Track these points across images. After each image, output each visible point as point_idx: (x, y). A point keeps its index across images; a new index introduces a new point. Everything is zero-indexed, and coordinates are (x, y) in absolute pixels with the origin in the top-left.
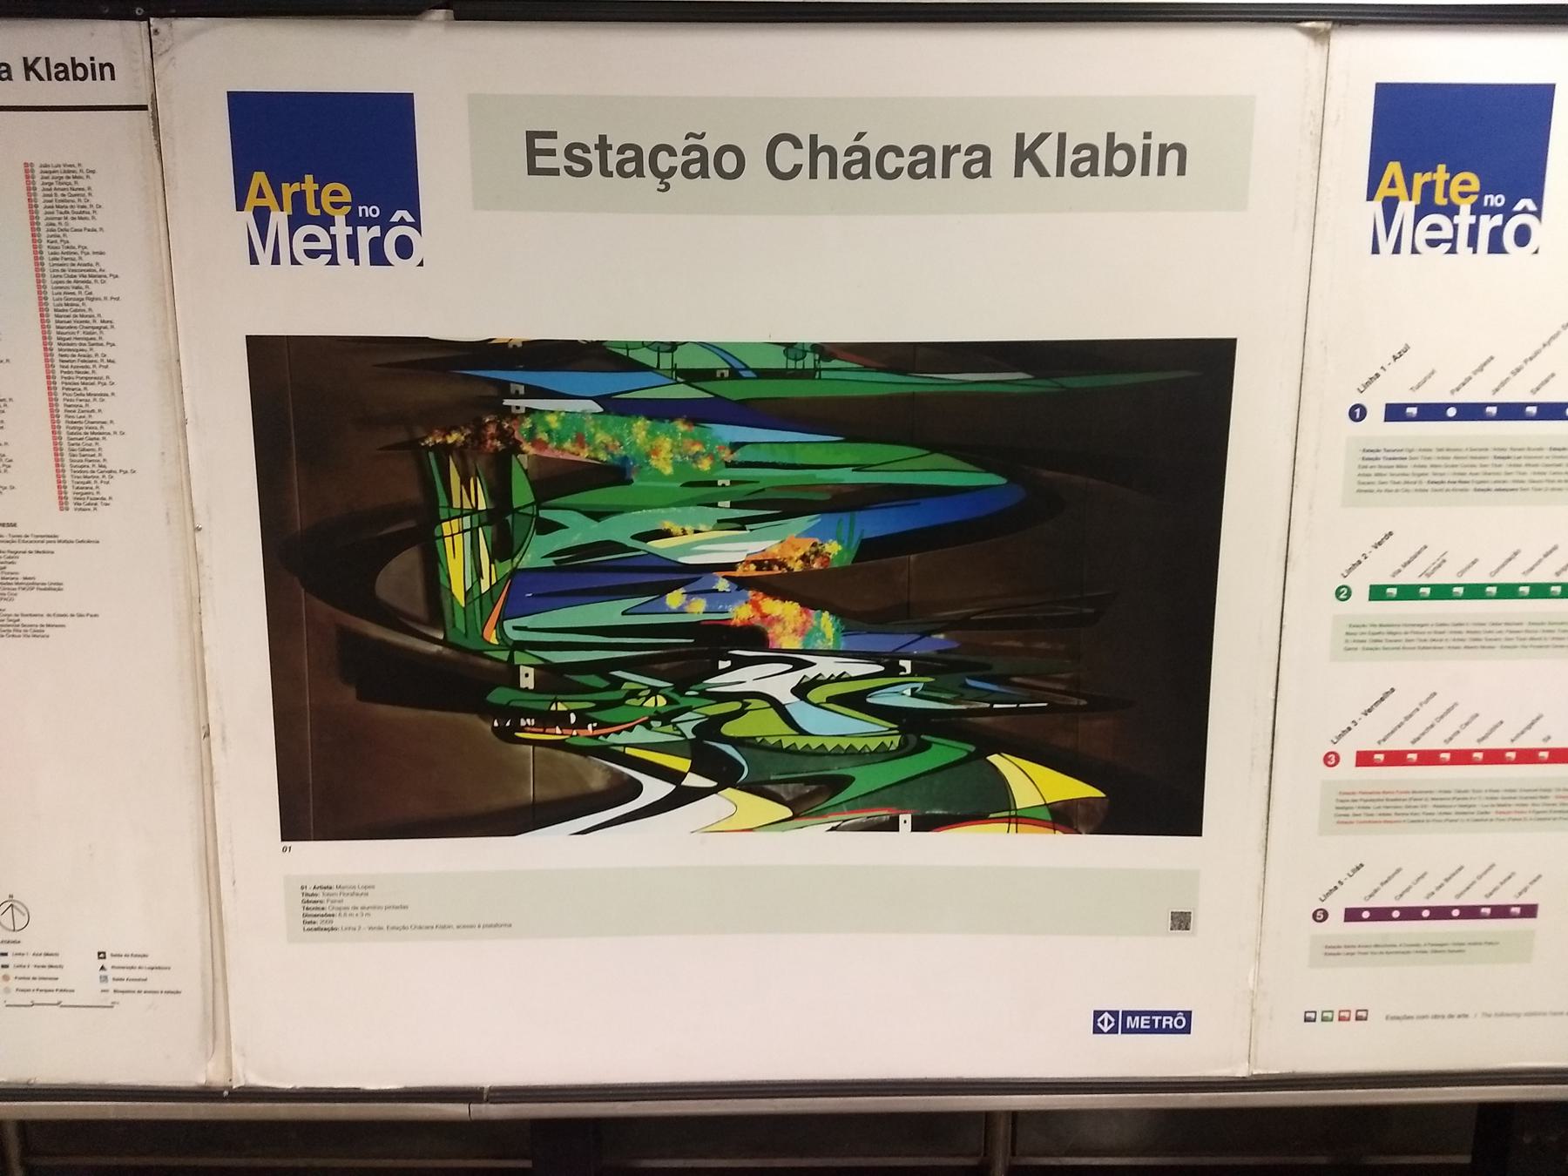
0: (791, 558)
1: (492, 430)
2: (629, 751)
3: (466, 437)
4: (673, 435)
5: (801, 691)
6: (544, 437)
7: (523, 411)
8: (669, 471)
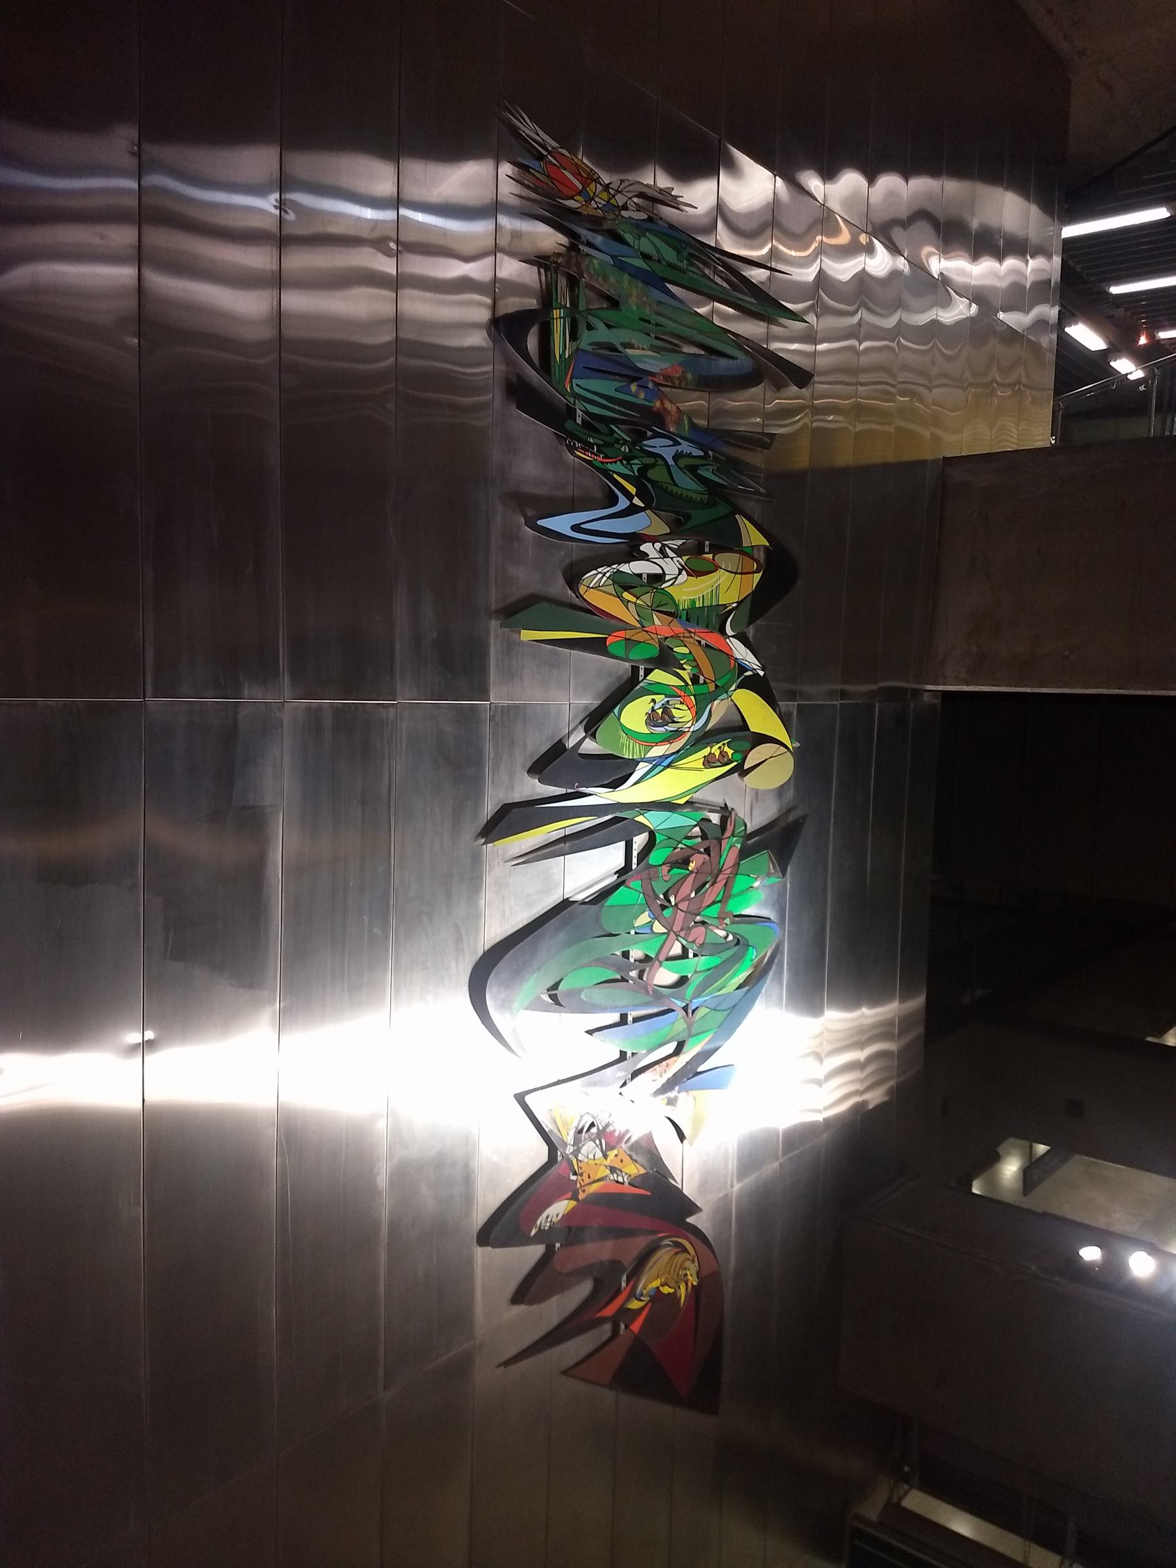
0: (674, 377)
1: (574, 260)
2: (615, 476)
5: (676, 457)
6: (592, 271)
7: (585, 253)
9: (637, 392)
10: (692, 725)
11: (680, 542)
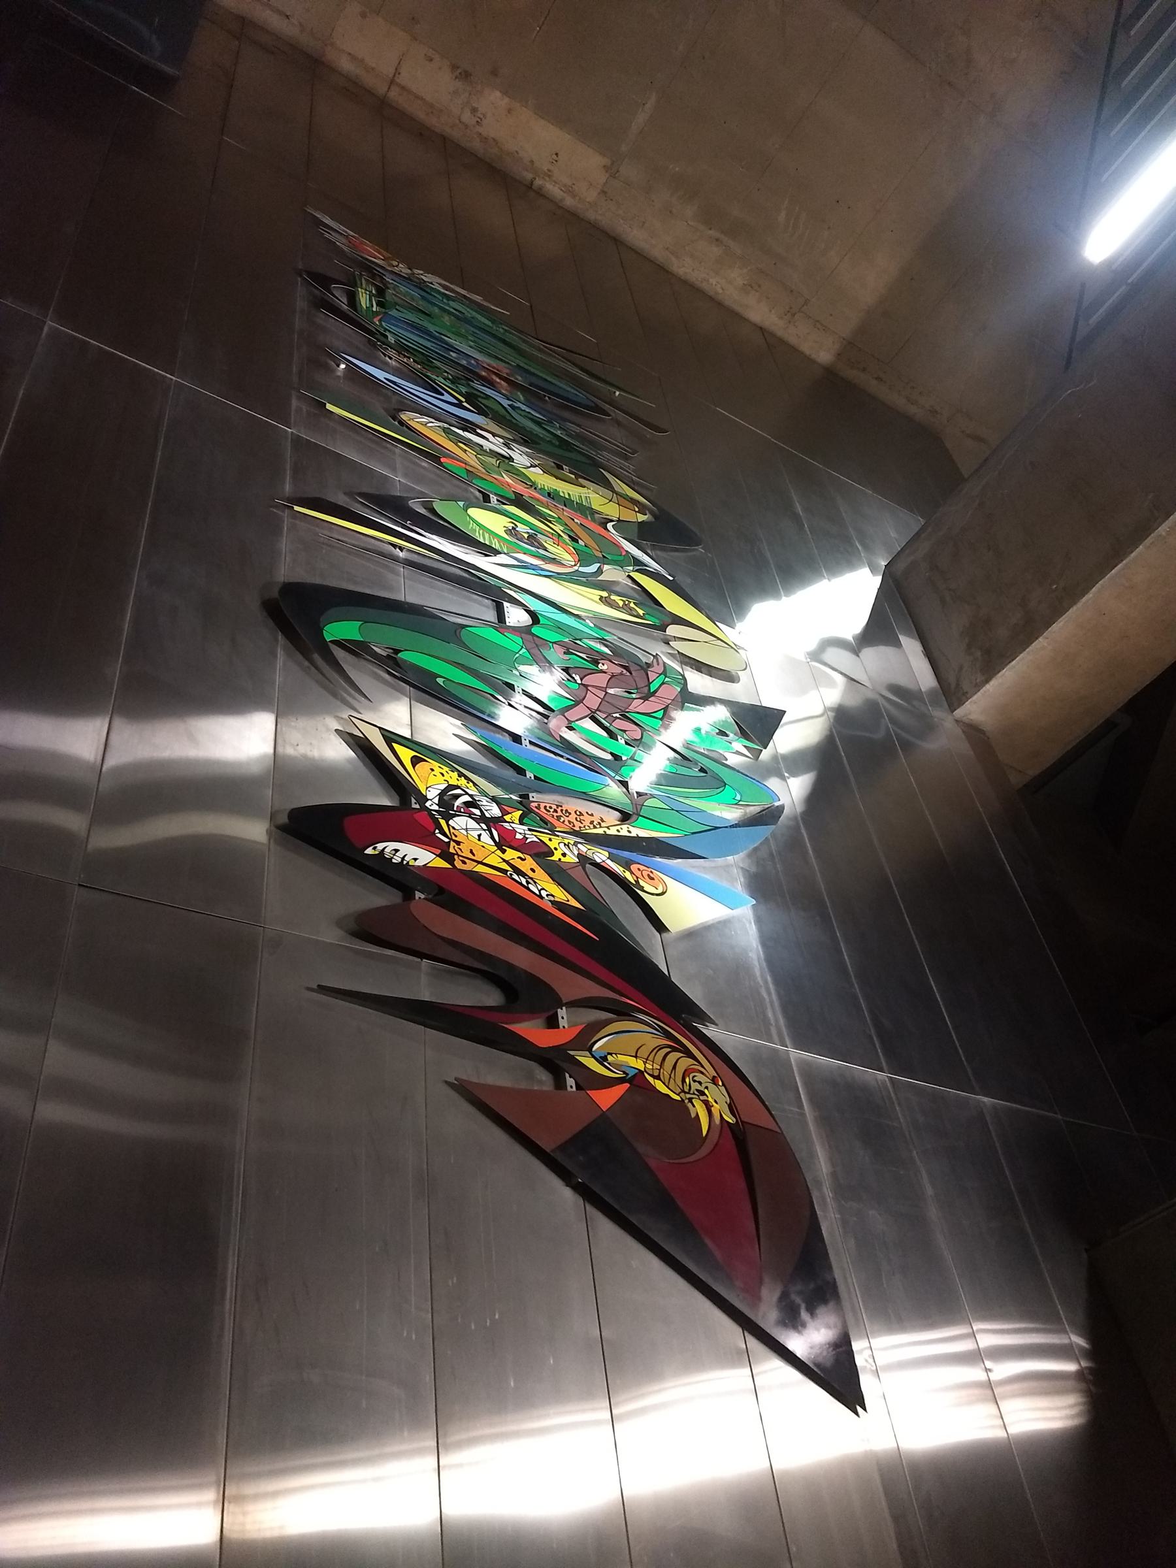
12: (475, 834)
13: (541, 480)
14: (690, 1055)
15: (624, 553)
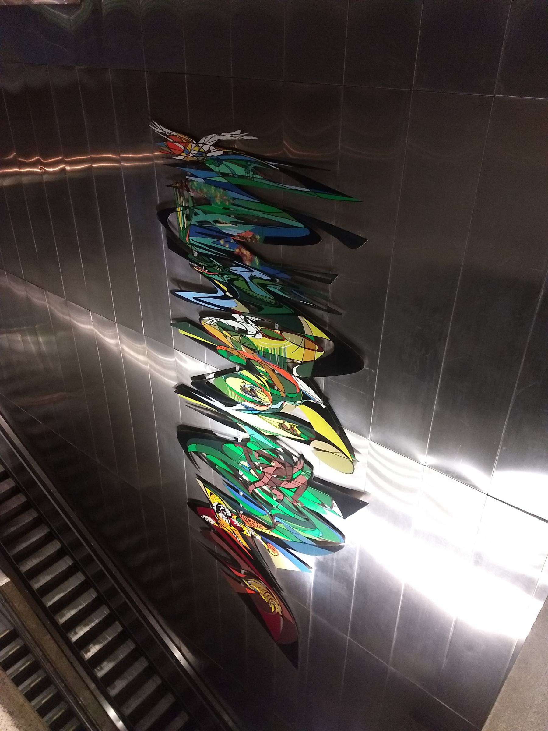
0: (248, 237)
1: (184, 184)
2: (215, 280)
3: (180, 185)
4: (220, 192)
5: (251, 278)
6: (194, 188)
8: (219, 203)
9: (225, 244)
10: (270, 405)
11: (257, 319)
12: (224, 519)
13: (261, 344)
14: (273, 596)
15: (298, 391)
